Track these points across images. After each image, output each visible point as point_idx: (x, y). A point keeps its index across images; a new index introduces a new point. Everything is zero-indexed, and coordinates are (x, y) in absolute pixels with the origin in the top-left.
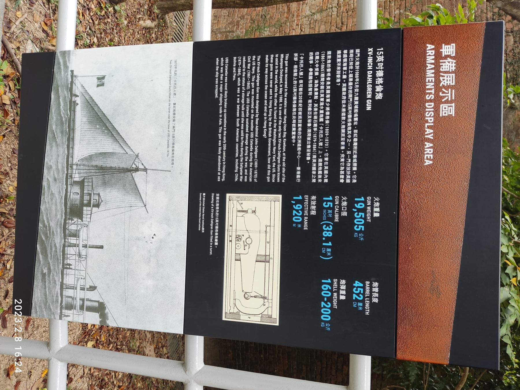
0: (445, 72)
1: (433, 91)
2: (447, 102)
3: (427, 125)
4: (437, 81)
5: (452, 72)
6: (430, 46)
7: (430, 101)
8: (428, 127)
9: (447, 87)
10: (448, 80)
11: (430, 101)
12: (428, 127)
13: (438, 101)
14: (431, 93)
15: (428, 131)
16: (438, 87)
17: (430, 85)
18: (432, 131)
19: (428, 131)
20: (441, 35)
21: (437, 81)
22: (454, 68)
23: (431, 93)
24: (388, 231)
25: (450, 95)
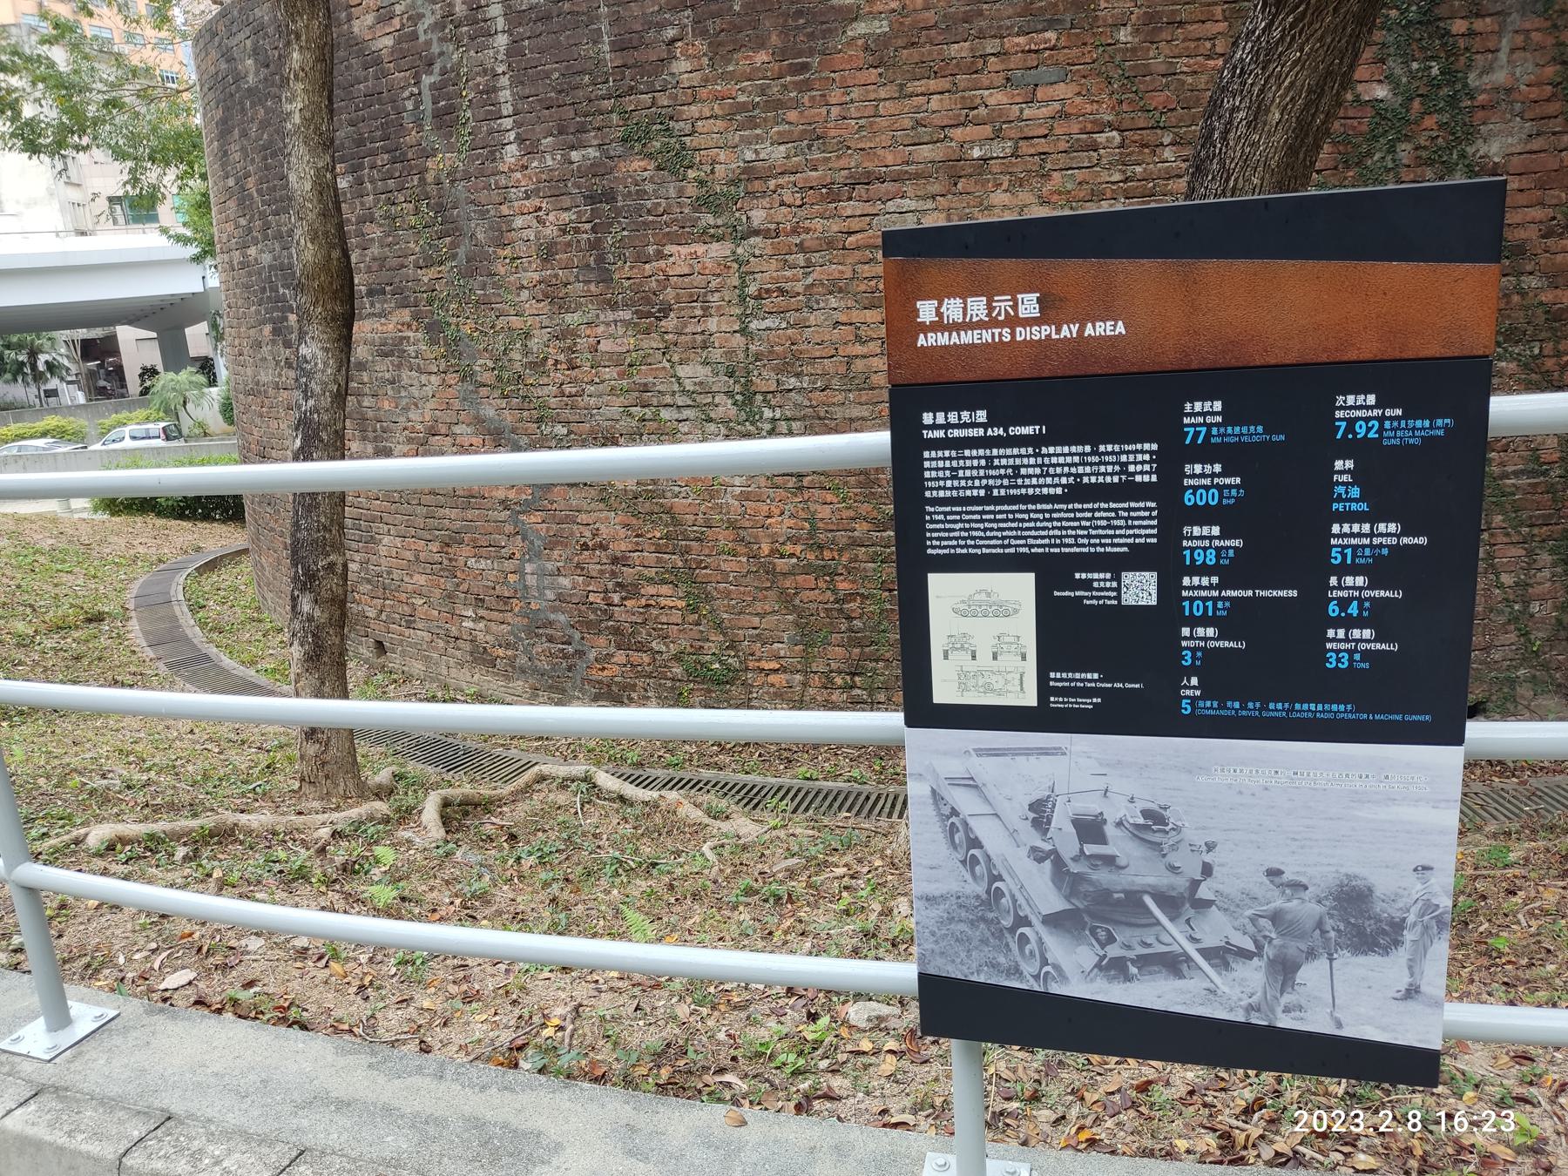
0: (965, 314)
1: (996, 331)
2: (1015, 307)
3: (1054, 336)
4: (981, 325)
5: (965, 303)
6: (921, 341)
7: (1013, 334)
8: (1058, 331)
9: (990, 308)
10: (978, 307)
11: (1013, 334)
12: (1058, 331)
13: (1013, 322)
14: (1000, 335)
15: (1065, 332)
16: (992, 323)
17: (987, 336)
18: (1065, 327)
19: (1065, 332)
20: (902, 327)
21: (981, 325)
22: (959, 301)
23: (1000, 335)
24: (1243, 385)
25: (1003, 304)
